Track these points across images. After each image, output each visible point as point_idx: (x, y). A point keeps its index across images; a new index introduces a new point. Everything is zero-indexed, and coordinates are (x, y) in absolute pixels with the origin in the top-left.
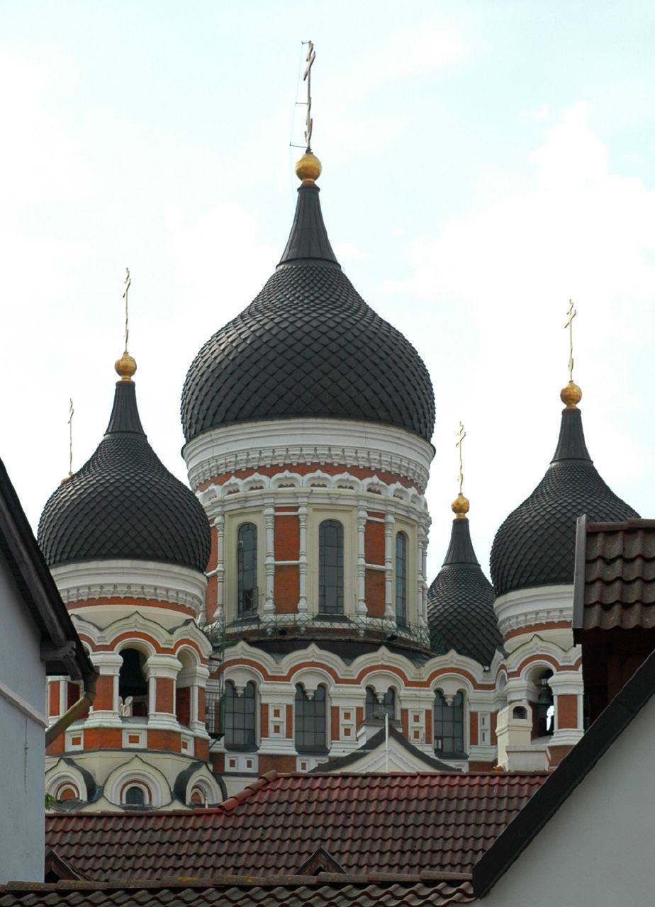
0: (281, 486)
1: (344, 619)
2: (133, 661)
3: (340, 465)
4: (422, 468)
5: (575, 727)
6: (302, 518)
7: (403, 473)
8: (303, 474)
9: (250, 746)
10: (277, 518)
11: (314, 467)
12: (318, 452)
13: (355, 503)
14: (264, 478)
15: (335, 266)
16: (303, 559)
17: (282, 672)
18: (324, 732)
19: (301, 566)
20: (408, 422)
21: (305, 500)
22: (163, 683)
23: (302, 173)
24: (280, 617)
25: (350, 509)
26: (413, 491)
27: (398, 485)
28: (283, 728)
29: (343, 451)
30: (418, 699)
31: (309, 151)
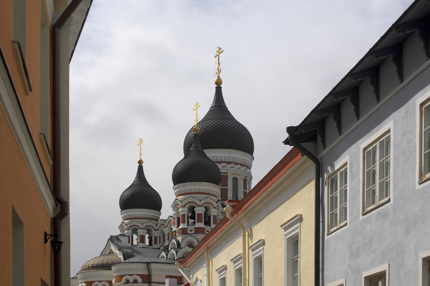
0: (222, 167)
3: (231, 162)
4: (250, 162)
5: (202, 223)
6: (229, 176)
7: (247, 165)
13: (241, 173)
15: (226, 109)
16: (229, 187)
19: (228, 189)
23: (216, 83)
25: (240, 174)
26: (249, 170)
27: (245, 167)
29: (232, 158)
31: (219, 77)
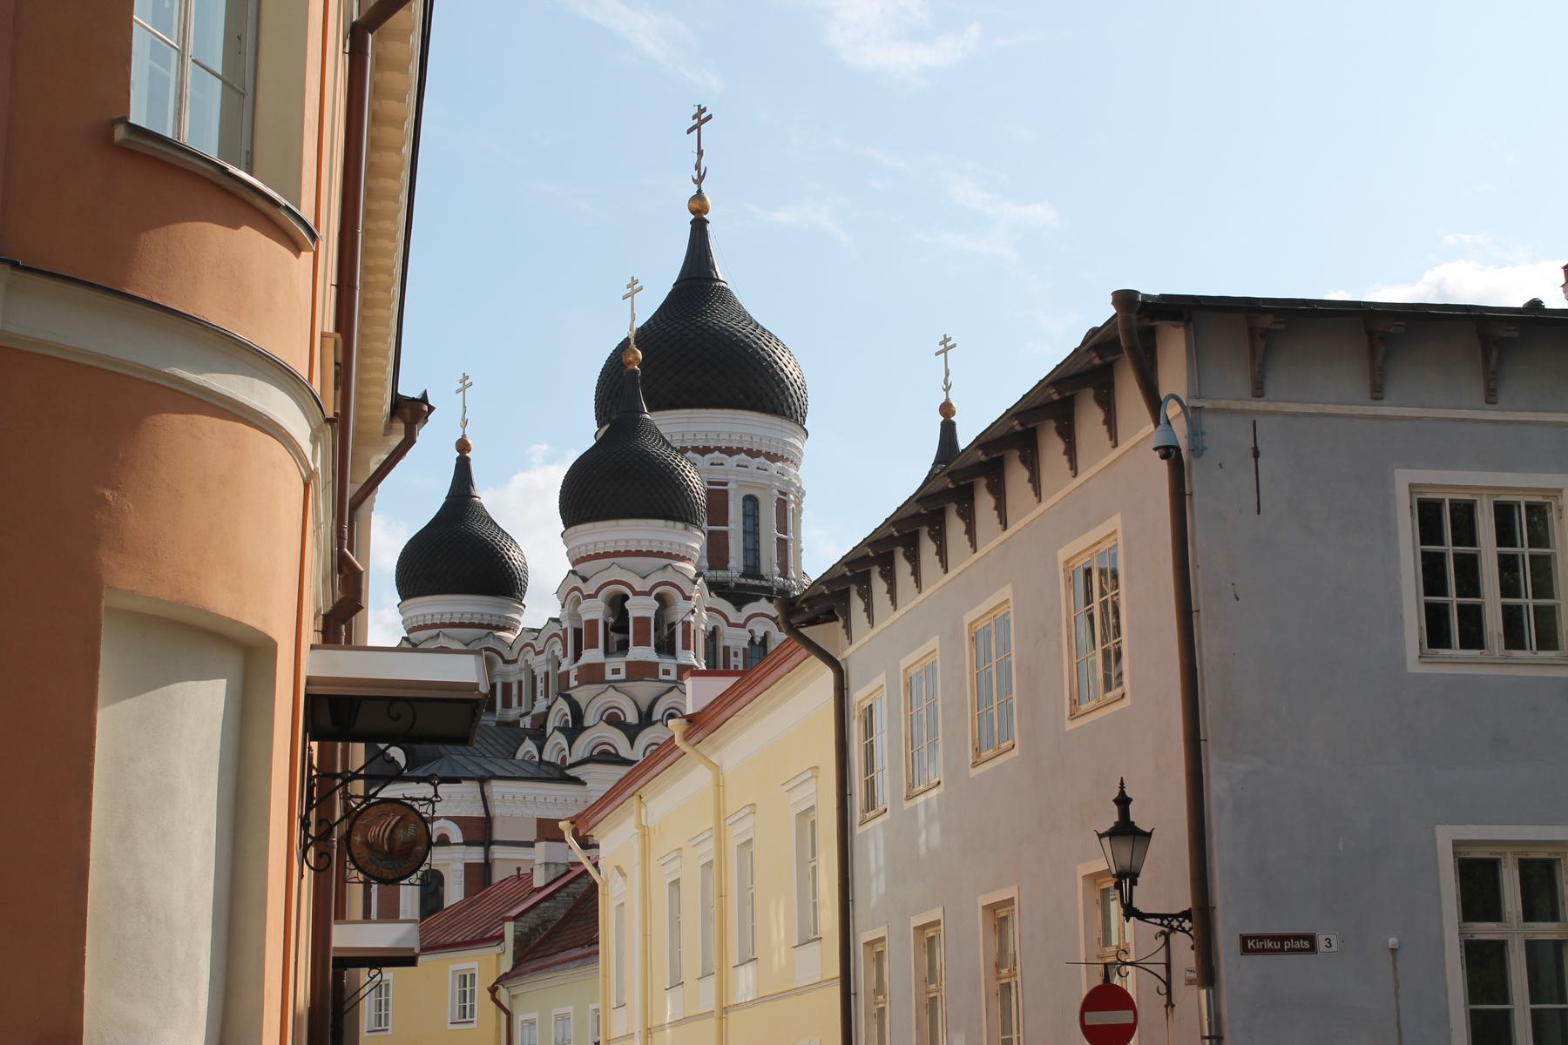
0: (712, 464)
1: (761, 578)
2: (618, 604)
8: (730, 456)
11: (739, 451)
12: (697, 438)
20: (788, 413)
21: (734, 477)
22: (642, 622)
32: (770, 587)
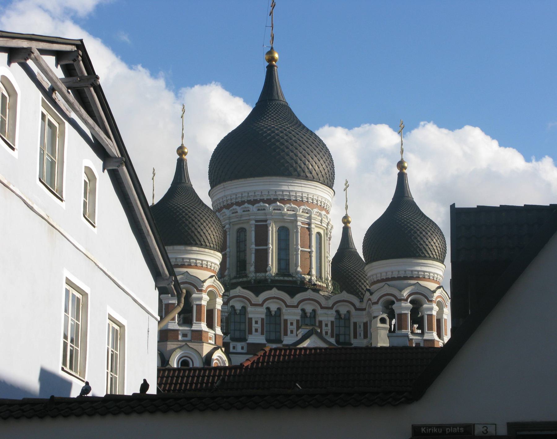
0: (259, 210)
1: (290, 275)
9: (244, 339)
10: (256, 226)
14: (250, 206)
17: (259, 302)
18: (280, 332)
24: (258, 274)
28: (260, 330)
30: (327, 315)
32: (295, 281)
